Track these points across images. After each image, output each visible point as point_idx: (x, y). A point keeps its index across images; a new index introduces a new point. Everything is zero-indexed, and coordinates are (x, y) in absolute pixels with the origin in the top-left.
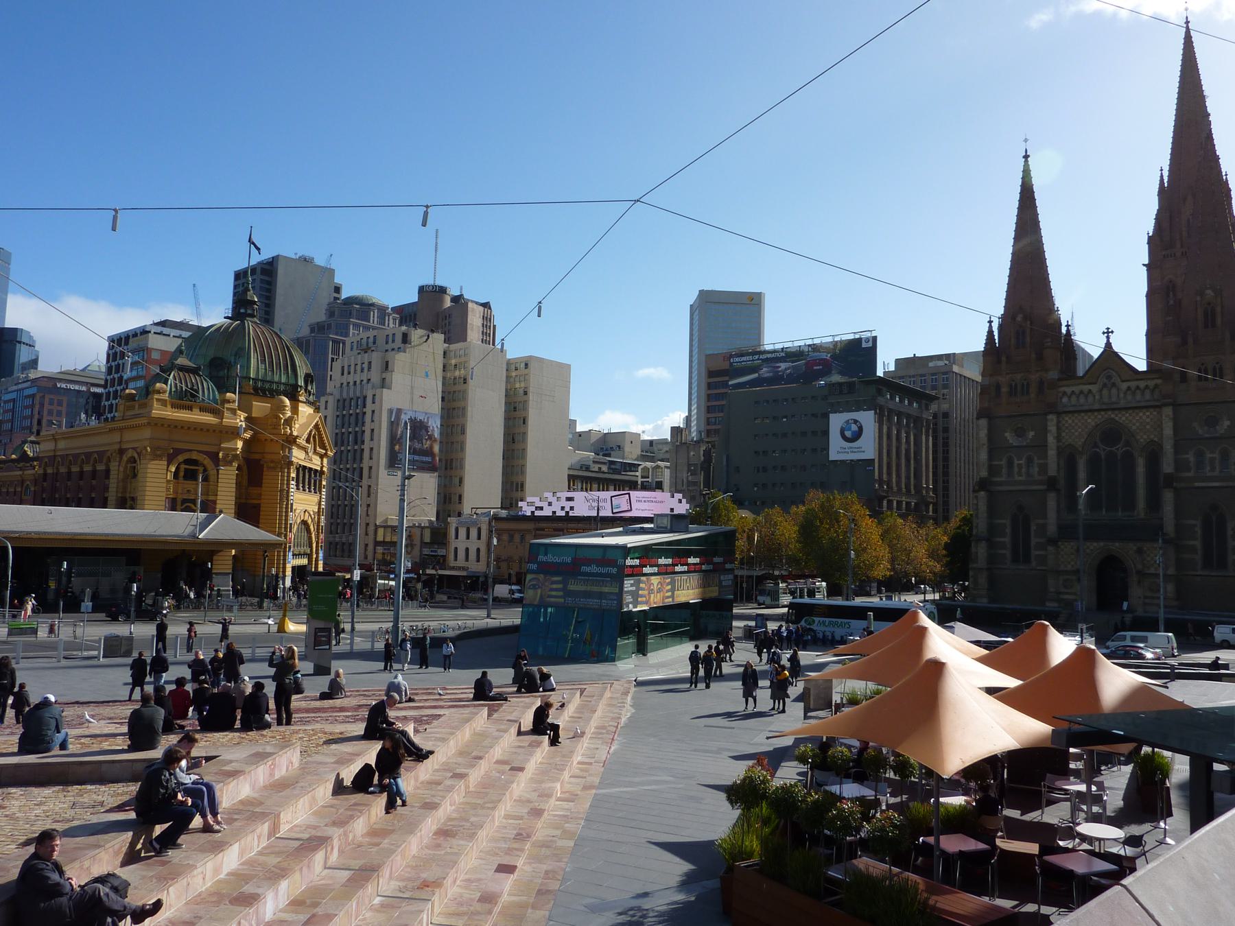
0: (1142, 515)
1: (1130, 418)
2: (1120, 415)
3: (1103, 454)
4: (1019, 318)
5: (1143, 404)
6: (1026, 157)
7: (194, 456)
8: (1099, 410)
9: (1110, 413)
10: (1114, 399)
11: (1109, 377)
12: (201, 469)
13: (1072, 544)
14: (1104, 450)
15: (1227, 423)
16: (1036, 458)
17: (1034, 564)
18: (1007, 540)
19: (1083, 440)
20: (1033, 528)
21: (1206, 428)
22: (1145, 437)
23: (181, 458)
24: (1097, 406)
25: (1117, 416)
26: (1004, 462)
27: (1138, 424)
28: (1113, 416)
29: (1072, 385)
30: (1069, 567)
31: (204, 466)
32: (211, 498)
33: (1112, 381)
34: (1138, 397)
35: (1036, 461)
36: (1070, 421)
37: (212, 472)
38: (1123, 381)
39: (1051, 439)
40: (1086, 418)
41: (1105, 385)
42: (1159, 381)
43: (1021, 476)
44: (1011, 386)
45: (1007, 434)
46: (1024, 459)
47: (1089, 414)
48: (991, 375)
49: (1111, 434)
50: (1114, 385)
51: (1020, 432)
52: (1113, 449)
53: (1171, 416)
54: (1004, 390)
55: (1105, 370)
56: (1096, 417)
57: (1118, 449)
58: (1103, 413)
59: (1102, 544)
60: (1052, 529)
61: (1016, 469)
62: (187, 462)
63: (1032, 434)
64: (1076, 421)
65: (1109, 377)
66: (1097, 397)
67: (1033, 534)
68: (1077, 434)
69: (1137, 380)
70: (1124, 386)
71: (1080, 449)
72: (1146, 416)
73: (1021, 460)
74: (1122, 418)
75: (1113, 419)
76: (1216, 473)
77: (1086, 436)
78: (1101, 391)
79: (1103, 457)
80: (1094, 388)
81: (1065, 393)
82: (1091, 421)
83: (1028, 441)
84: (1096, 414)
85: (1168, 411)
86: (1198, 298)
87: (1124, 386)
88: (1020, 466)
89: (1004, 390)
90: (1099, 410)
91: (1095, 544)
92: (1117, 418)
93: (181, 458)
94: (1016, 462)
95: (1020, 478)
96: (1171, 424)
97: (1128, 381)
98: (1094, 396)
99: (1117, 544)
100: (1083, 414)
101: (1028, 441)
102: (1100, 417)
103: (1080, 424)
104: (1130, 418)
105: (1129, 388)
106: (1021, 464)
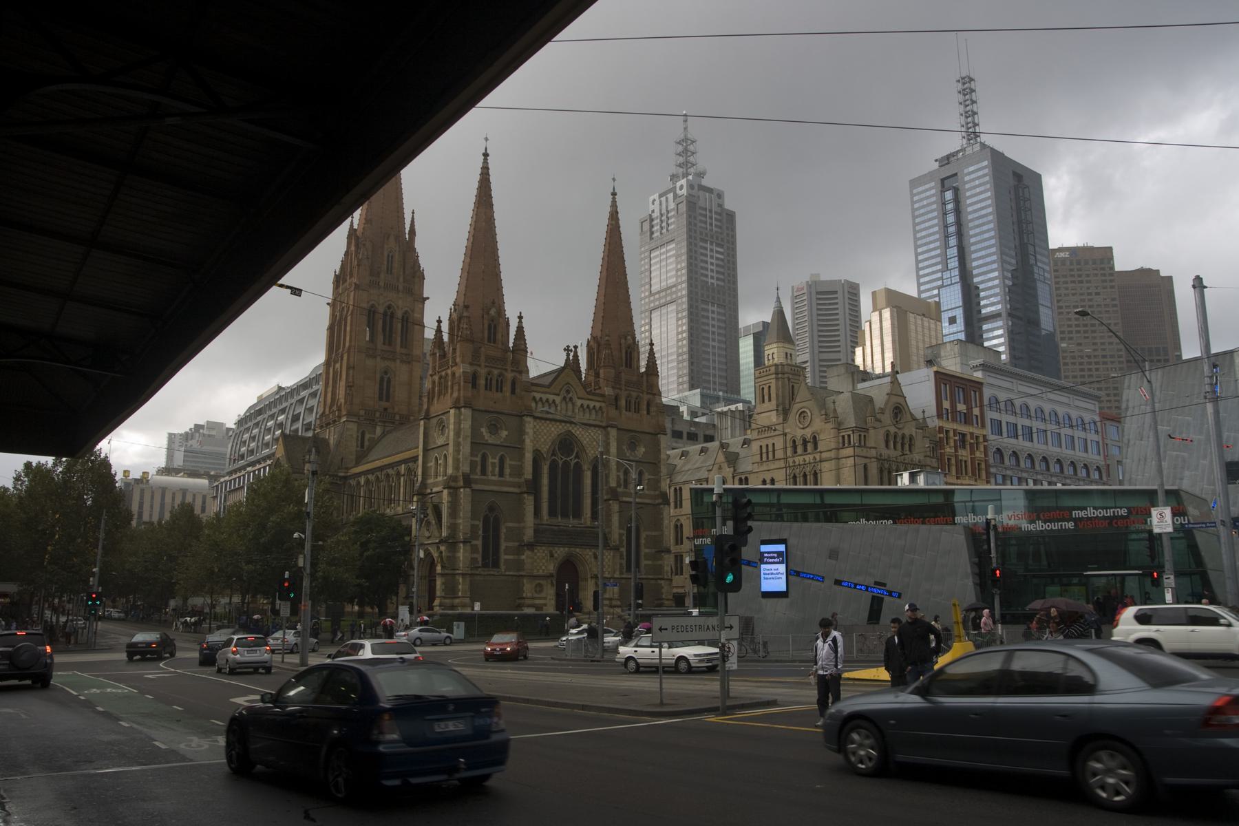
0: (589, 523)
1: (583, 433)
2: (575, 429)
3: (560, 462)
4: (493, 312)
5: (591, 422)
6: (486, 155)
8: (561, 421)
9: (568, 425)
10: (570, 413)
11: (568, 392)
13: (544, 548)
14: (562, 459)
15: (644, 450)
16: (508, 459)
17: (503, 567)
18: (479, 543)
19: (547, 447)
20: (503, 530)
21: (629, 451)
22: (592, 452)
24: (558, 417)
25: (573, 428)
26: (478, 459)
27: (587, 440)
28: (570, 428)
29: (542, 393)
30: (541, 572)
33: (570, 395)
34: (587, 415)
35: (508, 462)
36: (538, 427)
38: (579, 398)
39: (528, 441)
40: (551, 426)
41: (564, 398)
42: (603, 405)
43: (495, 475)
44: (487, 379)
45: (483, 430)
46: (498, 458)
47: (553, 423)
48: (471, 364)
49: (567, 444)
50: (571, 399)
51: (494, 429)
52: (568, 459)
53: (616, 437)
54: (482, 382)
55: (567, 384)
56: (558, 426)
57: (571, 460)
58: (563, 424)
59: (567, 549)
60: (529, 535)
61: (490, 468)
63: (504, 433)
64: (543, 427)
65: (568, 392)
66: (559, 408)
67: (503, 536)
68: (542, 440)
69: (589, 400)
70: (579, 402)
71: (545, 455)
72: (598, 434)
73: (496, 459)
74: (578, 431)
75: (570, 431)
77: (550, 444)
78: (561, 403)
79: (560, 466)
80: (558, 399)
81: (534, 398)
82: (555, 430)
83: (502, 440)
84: (558, 424)
85: (613, 433)
86: (623, 341)
87: (579, 402)
88: (493, 464)
89: (482, 382)
90: (561, 421)
91: (562, 549)
92: (573, 431)
94: (490, 460)
95: (493, 478)
96: (615, 444)
97: (582, 399)
98: (556, 406)
99: (578, 550)
100: (548, 422)
101: (502, 440)
102: (560, 427)
103: (545, 431)
104: (583, 433)
106: (495, 463)
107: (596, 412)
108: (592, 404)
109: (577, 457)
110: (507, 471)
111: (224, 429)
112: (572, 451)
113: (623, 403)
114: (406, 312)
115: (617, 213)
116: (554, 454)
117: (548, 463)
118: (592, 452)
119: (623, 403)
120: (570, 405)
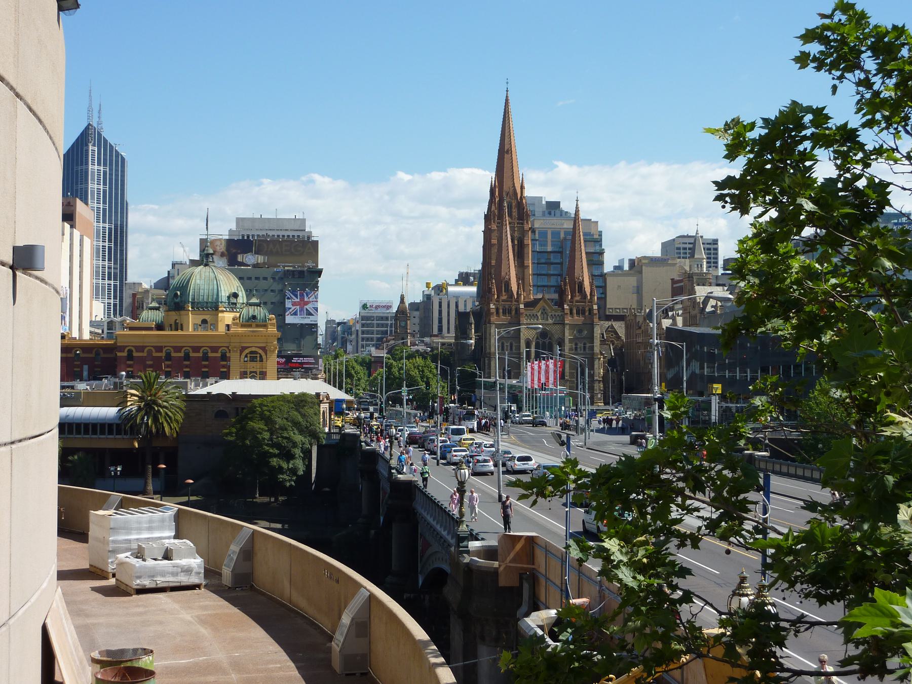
7: (254, 349)
12: (258, 355)
23: (247, 351)
31: (260, 354)
32: (264, 370)
35: (514, 344)
37: (264, 357)
41: (542, 313)
62: (252, 352)
72: (558, 327)
76: (582, 352)
81: (526, 315)
87: (550, 314)
93: (247, 351)
94: (505, 344)
105: (552, 315)
107: (560, 317)
108: (557, 314)
109: (550, 339)
110: (514, 348)
111: (544, 203)
112: (547, 336)
113: (575, 311)
114: (520, 238)
115: (578, 211)
116: (537, 338)
117: (534, 343)
118: (556, 337)
119: (575, 311)
120: (545, 315)
